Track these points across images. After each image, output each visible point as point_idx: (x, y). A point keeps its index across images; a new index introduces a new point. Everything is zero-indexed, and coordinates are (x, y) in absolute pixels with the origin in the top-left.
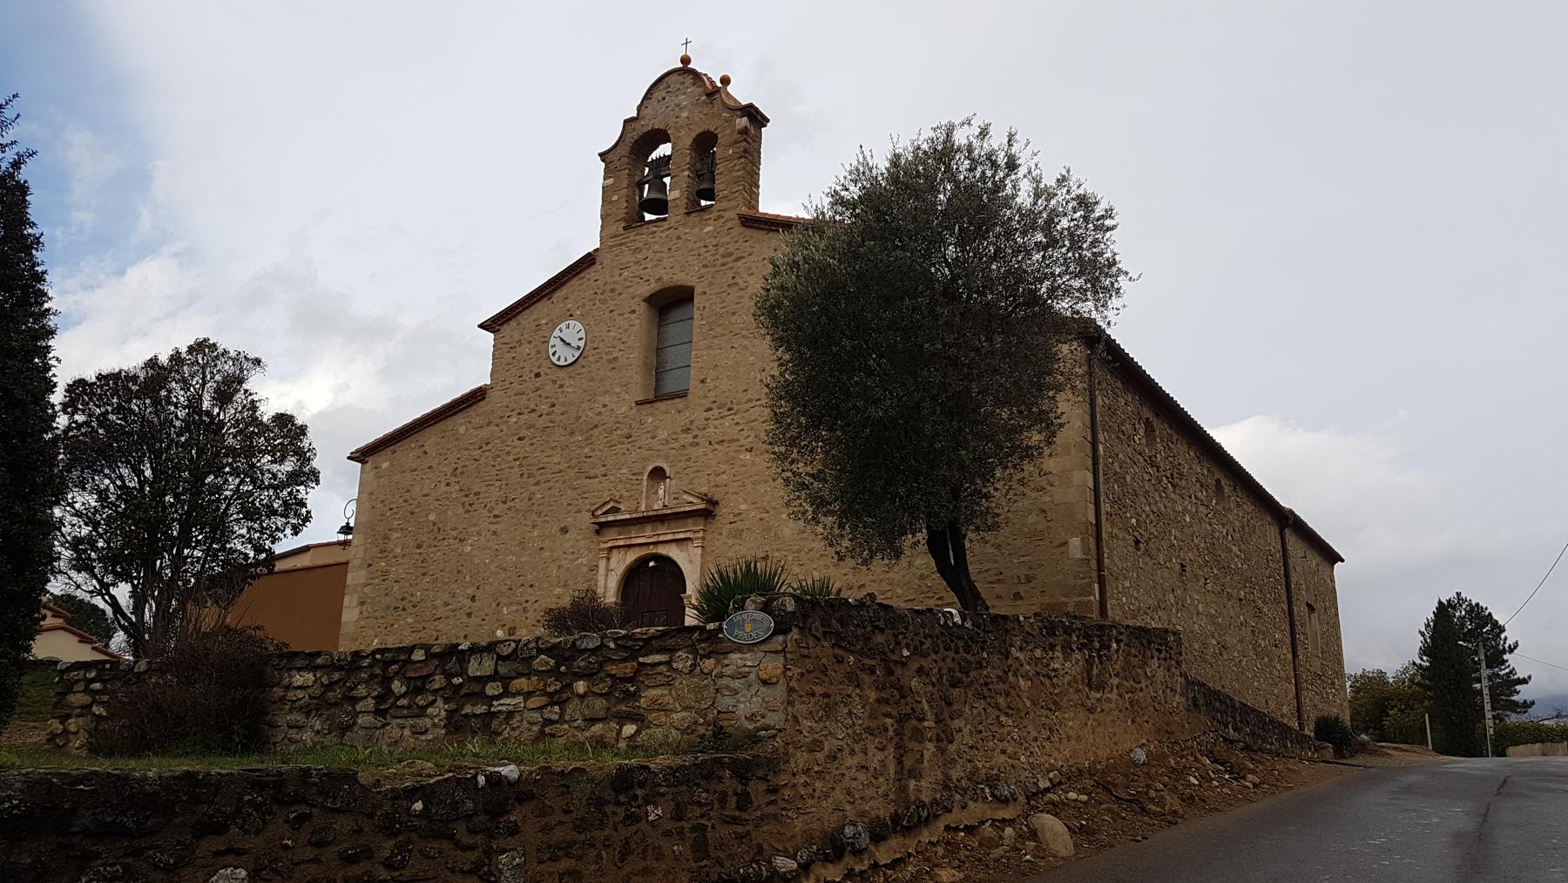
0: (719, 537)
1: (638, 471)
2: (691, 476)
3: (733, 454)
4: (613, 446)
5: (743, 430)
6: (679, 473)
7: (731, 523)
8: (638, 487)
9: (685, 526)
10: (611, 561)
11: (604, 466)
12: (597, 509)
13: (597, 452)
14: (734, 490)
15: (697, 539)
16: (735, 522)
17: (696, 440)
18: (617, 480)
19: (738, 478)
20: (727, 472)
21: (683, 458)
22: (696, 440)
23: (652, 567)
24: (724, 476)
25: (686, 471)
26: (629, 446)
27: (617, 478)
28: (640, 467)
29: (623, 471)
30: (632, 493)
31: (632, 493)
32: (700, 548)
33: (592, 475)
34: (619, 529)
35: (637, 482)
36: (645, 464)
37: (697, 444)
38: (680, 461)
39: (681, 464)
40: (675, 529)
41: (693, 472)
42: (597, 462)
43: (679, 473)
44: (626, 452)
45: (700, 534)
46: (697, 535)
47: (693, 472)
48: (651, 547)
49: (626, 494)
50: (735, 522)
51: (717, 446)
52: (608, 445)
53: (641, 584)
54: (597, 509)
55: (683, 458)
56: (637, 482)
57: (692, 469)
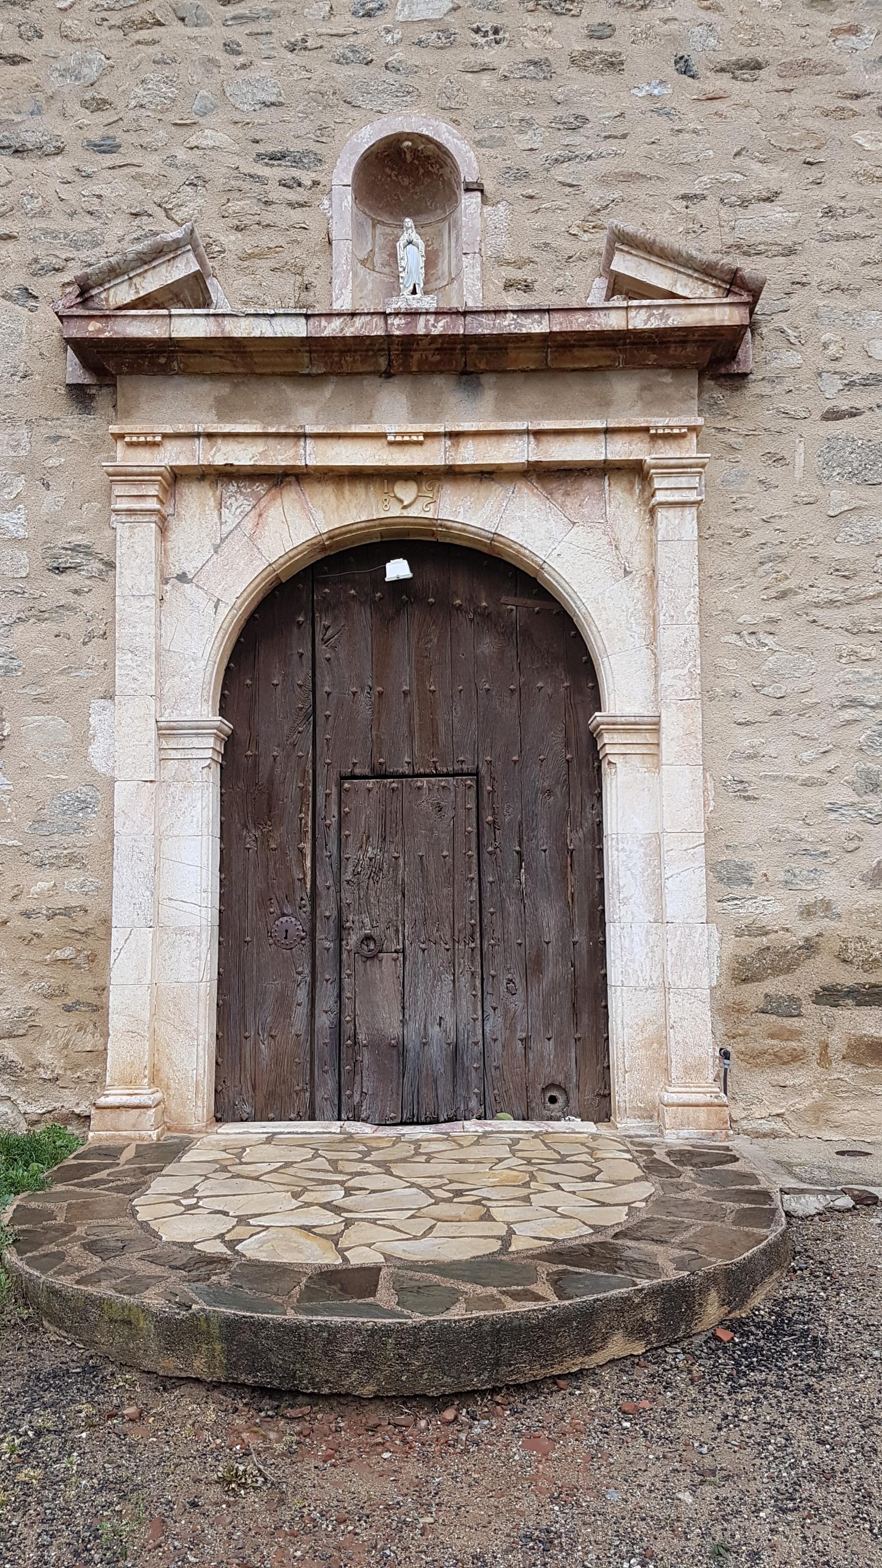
0: (776, 473)
1: (295, 146)
2: (595, 195)
3: (810, 123)
4: (143, 24)
5: (854, 30)
6: (522, 176)
7: (833, 415)
8: (297, 215)
9: (604, 404)
10: (179, 534)
11: (100, 105)
12: (114, 272)
13: (51, 43)
14: (833, 276)
15: (680, 468)
16: (853, 414)
17: (606, 47)
18: (178, 177)
19: (854, 224)
20: (791, 194)
21: (542, 117)
22: (606, 47)
23: (400, 583)
24: (775, 212)
25: (561, 173)
26: (238, 33)
27: (171, 161)
28: (306, 126)
29: (209, 137)
30: (267, 239)
31: (267, 239)
32: (690, 514)
33: (31, 139)
34: (223, 389)
35: (293, 196)
36: (327, 118)
37: (614, 64)
38: (526, 123)
39: (524, 140)
40: (544, 416)
41: (604, 180)
42: (55, 83)
43: (522, 176)
44: (221, 56)
45: (688, 450)
46: (668, 452)
47: (604, 180)
48: (406, 492)
49: (230, 240)
50: (853, 414)
51: (723, 82)
52: (116, 18)
53: (325, 653)
54: (114, 272)
55: (542, 117)
56: (293, 196)
57: (601, 166)
